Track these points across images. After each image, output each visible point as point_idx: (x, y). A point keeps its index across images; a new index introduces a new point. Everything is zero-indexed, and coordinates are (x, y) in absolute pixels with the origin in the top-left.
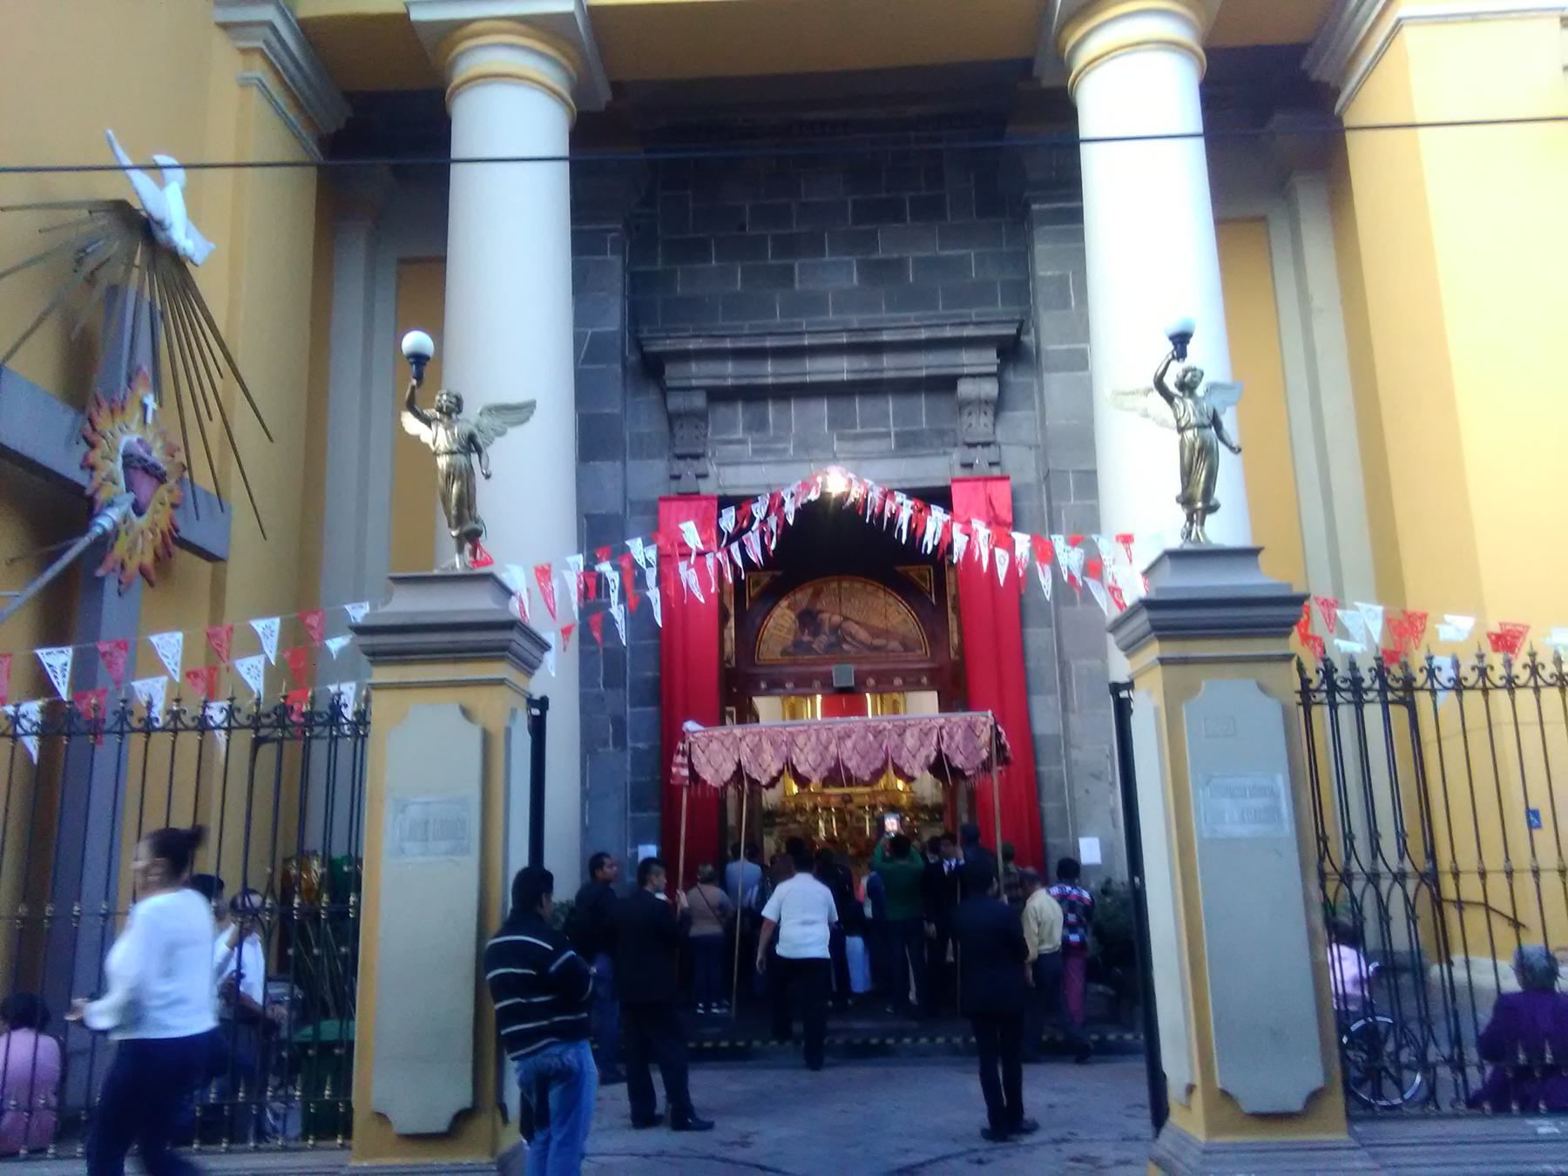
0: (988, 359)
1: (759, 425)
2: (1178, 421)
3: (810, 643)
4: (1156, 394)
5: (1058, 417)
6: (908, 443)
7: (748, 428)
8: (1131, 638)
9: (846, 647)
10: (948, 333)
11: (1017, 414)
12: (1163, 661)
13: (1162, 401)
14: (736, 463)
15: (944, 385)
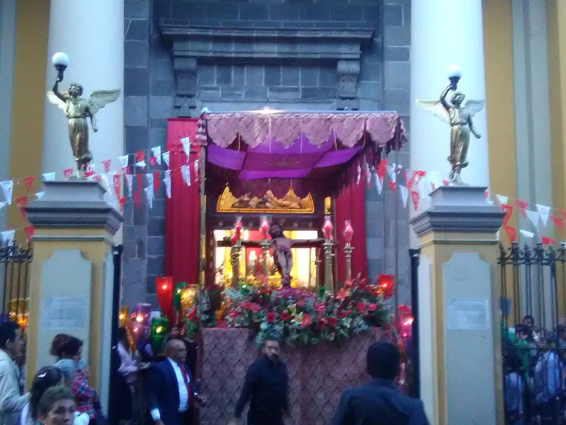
0: (355, 51)
1: (226, 80)
2: (451, 120)
3: (248, 201)
4: (441, 105)
5: (390, 87)
6: (309, 96)
7: (219, 81)
8: (422, 228)
9: (268, 204)
10: (334, 35)
11: (369, 82)
12: (435, 242)
13: (443, 109)
14: (212, 101)
15: (330, 64)
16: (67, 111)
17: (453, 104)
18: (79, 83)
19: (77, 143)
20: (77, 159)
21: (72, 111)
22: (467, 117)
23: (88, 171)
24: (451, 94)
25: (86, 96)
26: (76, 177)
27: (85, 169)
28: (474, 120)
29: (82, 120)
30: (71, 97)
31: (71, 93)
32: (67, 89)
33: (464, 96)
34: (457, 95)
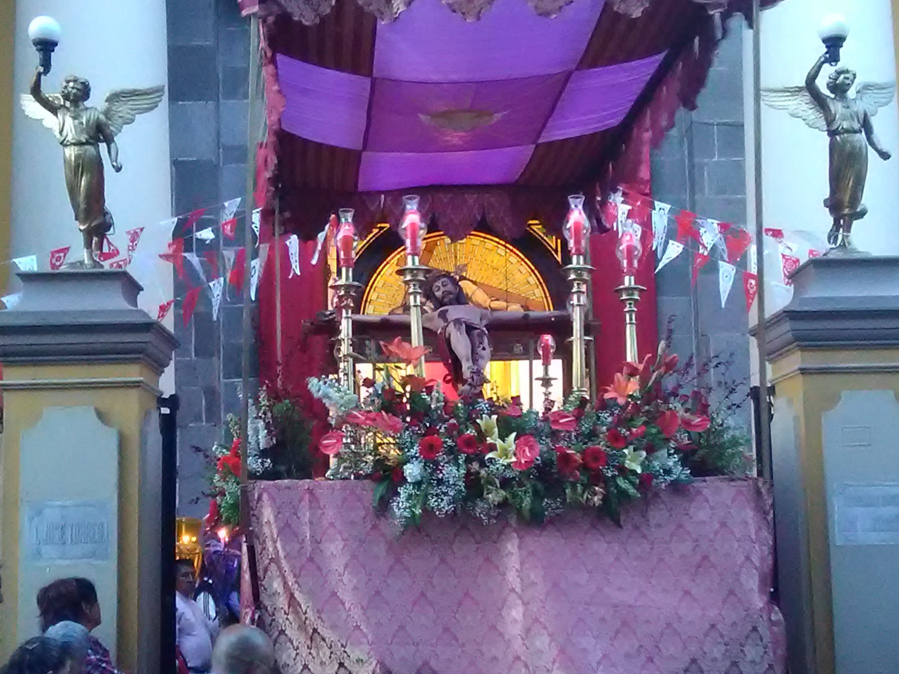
4: (806, 97)
16: (61, 132)
17: (832, 92)
18: (83, 76)
19: (81, 198)
20: (82, 228)
21: (70, 133)
22: (861, 117)
23: (106, 249)
24: (828, 71)
25: (97, 102)
26: (82, 263)
27: (100, 246)
28: (874, 121)
29: (90, 149)
30: (68, 104)
31: (66, 97)
32: (60, 89)
33: (855, 75)
34: (839, 73)
